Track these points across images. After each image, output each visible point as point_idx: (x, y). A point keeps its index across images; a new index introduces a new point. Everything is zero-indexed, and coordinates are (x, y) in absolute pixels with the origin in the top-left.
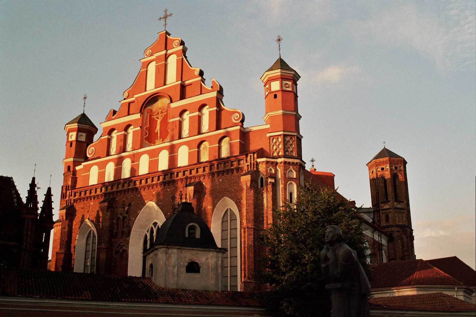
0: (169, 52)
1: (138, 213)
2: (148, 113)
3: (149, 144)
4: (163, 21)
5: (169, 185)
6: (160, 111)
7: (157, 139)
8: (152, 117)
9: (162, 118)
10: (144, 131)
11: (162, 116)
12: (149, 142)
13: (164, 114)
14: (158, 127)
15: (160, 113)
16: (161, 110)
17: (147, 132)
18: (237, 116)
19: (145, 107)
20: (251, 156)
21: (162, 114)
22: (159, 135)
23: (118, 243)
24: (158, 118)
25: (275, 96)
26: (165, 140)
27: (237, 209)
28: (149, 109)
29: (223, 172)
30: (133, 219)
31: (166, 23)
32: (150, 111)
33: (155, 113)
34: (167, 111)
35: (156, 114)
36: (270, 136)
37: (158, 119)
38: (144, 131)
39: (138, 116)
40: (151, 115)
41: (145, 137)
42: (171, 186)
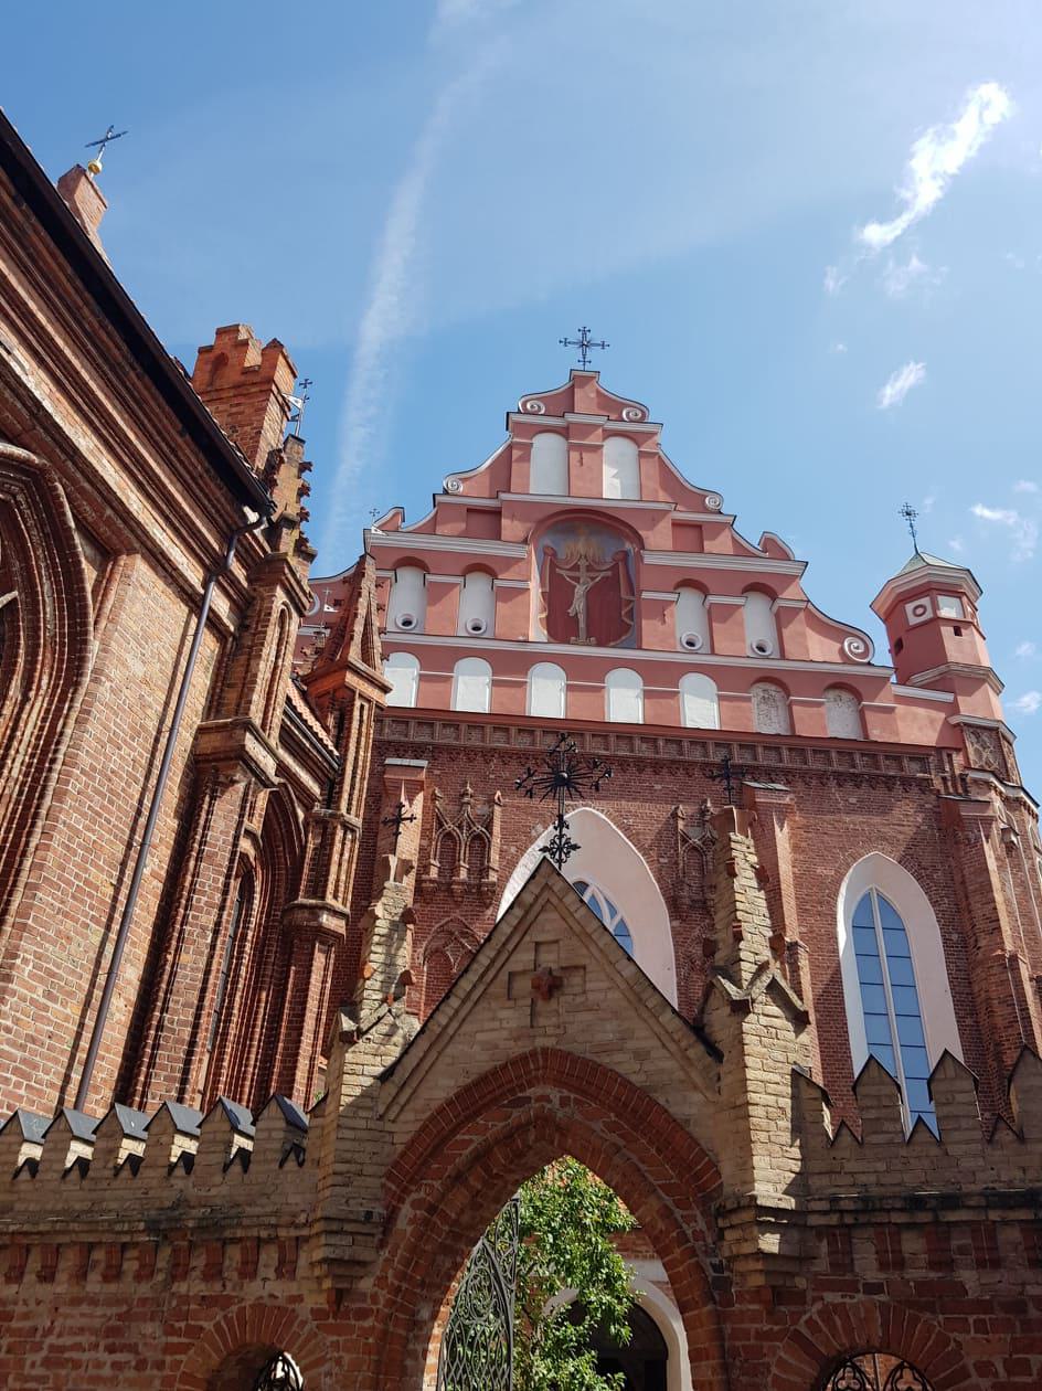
1: (534, 833)
2: (545, 554)
4: (577, 352)
5: (656, 773)
6: (583, 563)
9: (591, 584)
11: (593, 579)
13: (602, 574)
15: (583, 569)
18: (857, 648)
20: (950, 756)
21: (592, 575)
22: (582, 625)
23: (443, 922)
24: (577, 579)
25: (958, 632)
27: (926, 897)
29: (857, 780)
30: (513, 850)
32: (550, 552)
34: (615, 568)
35: (568, 567)
36: (965, 724)
37: (579, 582)
40: (553, 566)
42: (668, 778)
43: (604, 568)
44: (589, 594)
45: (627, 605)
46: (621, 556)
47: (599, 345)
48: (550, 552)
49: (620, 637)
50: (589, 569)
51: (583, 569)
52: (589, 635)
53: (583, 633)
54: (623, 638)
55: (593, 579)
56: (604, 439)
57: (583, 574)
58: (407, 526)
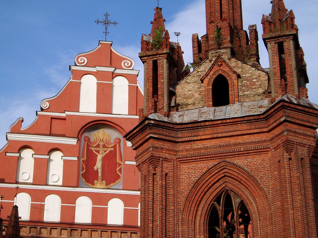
0: (118, 71)
2: (85, 141)
3: (87, 183)
4: (102, 27)
7: (97, 180)
8: (90, 148)
9: (104, 154)
10: (81, 165)
12: (85, 180)
14: (98, 165)
15: (101, 146)
16: (103, 142)
17: (84, 167)
19: (83, 133)
21: (105, 149)
22: (100, 175)
24: (98, 152)
26: (112, 184)
28: (86, 137)
31: (106, 31)
32: (87, 139)
33: (94, 144)
34: (115, 147)
37: (99, 153)
38: (81, 165)
39: (73, 142)
40: (88, 146)
41: (81, 173)
43: (111, 146)
44: (104, 159)
45: (119, 166)
46: (117, 141)
47: (113, 23)
48: (87, 139)
49: (115, 181)
50: (104, 146)
51: (101, 146)
52: (102, 180)
53: (100, 178)
54: (117, 182)
55: (105, 151)
56: (113, 78)
57: (101, 150)
58: (25, 126)
